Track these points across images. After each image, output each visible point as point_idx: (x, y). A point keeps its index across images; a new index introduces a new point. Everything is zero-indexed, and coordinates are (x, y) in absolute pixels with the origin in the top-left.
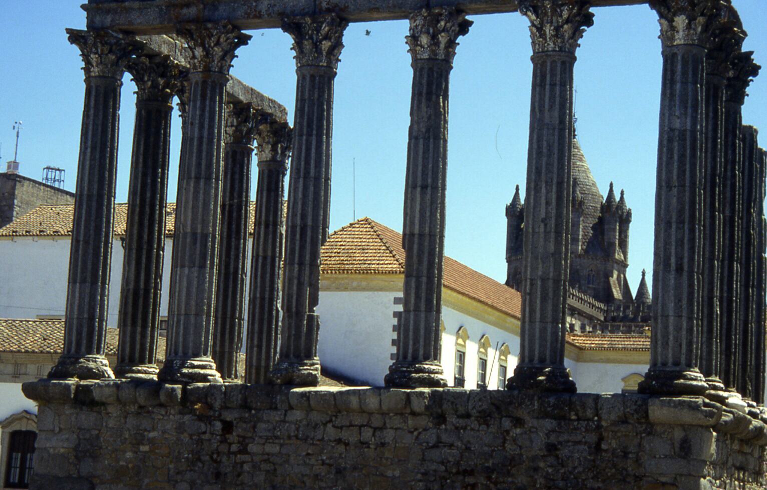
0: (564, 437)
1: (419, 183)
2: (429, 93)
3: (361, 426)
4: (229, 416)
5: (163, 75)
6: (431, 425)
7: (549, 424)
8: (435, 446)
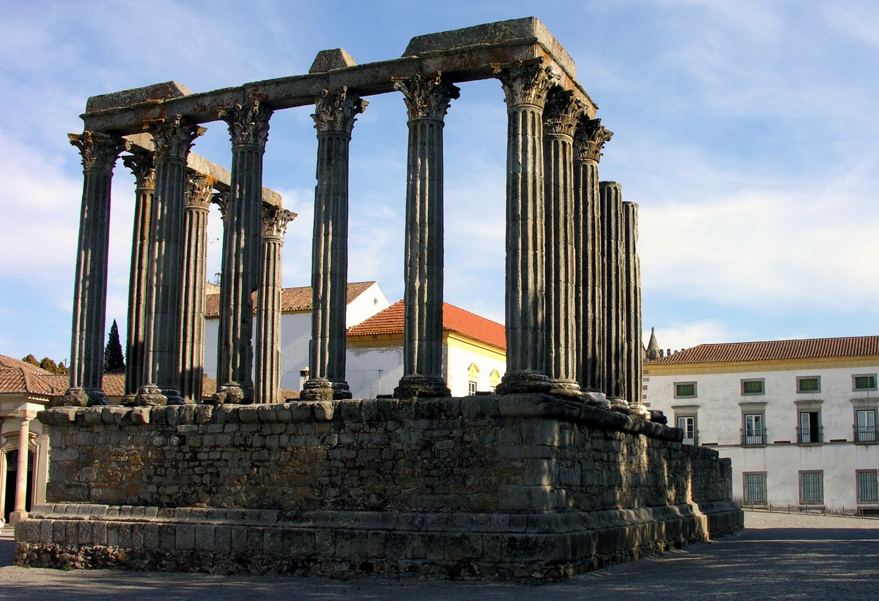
0: (436, 433)
2: (329, 159)
4: (182, 428)
6: (332, 430)
7: (423, 423)
8: (336, 447)
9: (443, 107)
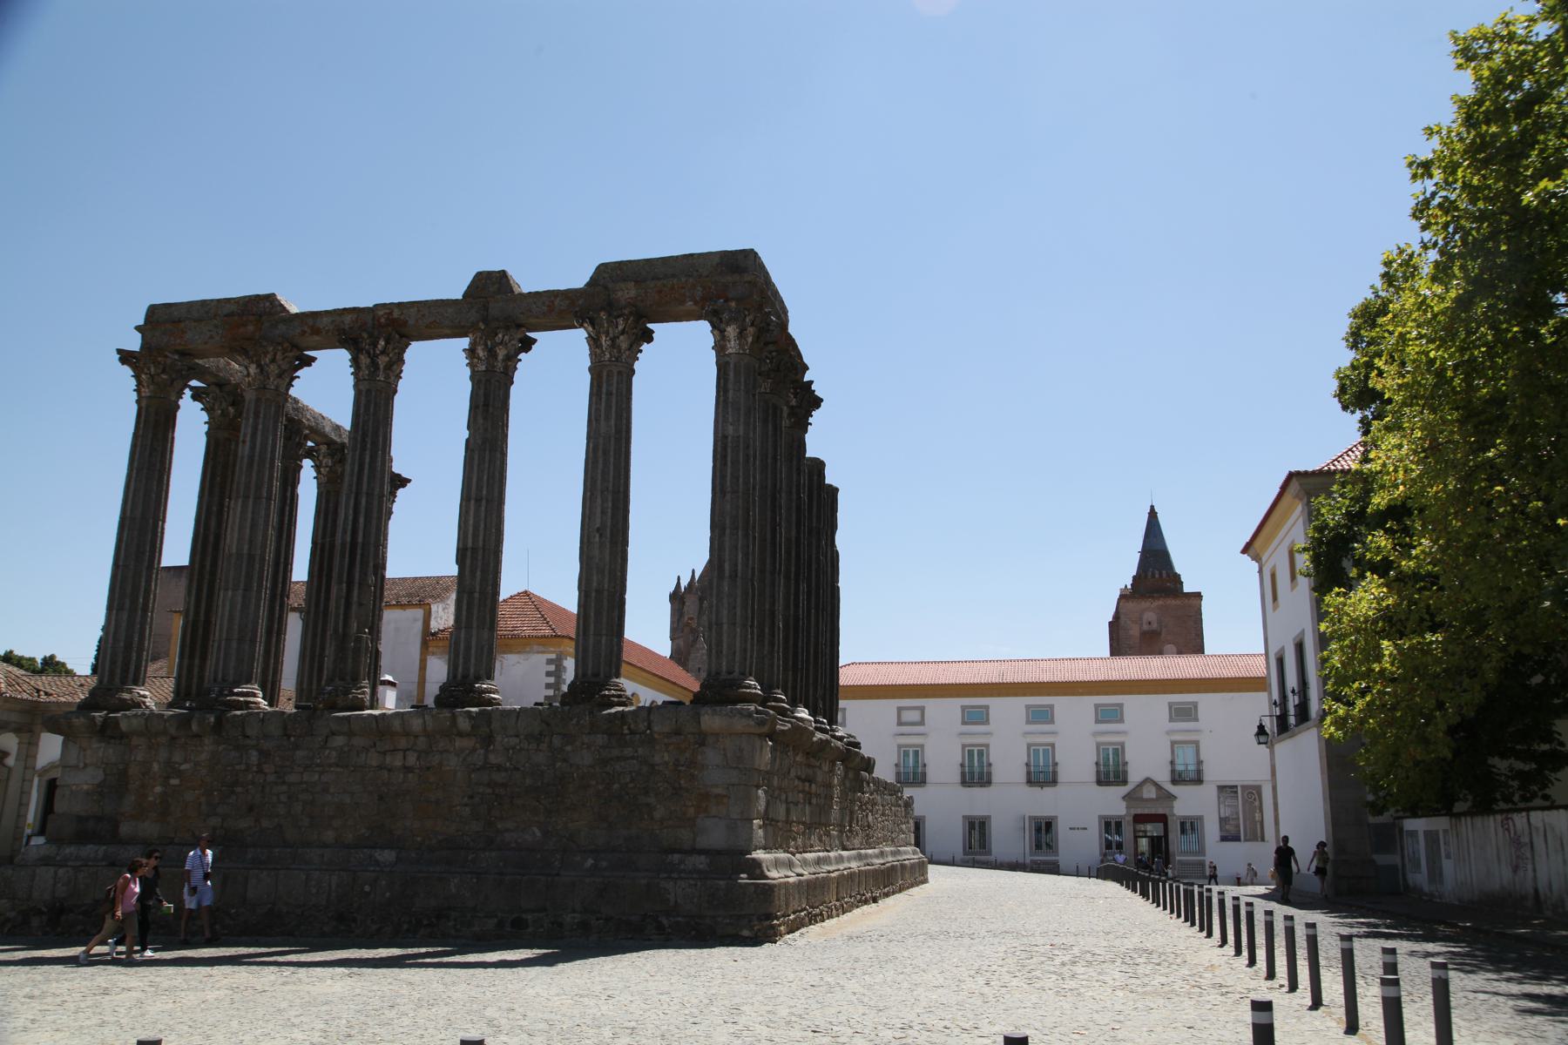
0: (616, 752)
2: (486, 405)
3: (405, 751)
5: (233, 404)
7: (600, 739)
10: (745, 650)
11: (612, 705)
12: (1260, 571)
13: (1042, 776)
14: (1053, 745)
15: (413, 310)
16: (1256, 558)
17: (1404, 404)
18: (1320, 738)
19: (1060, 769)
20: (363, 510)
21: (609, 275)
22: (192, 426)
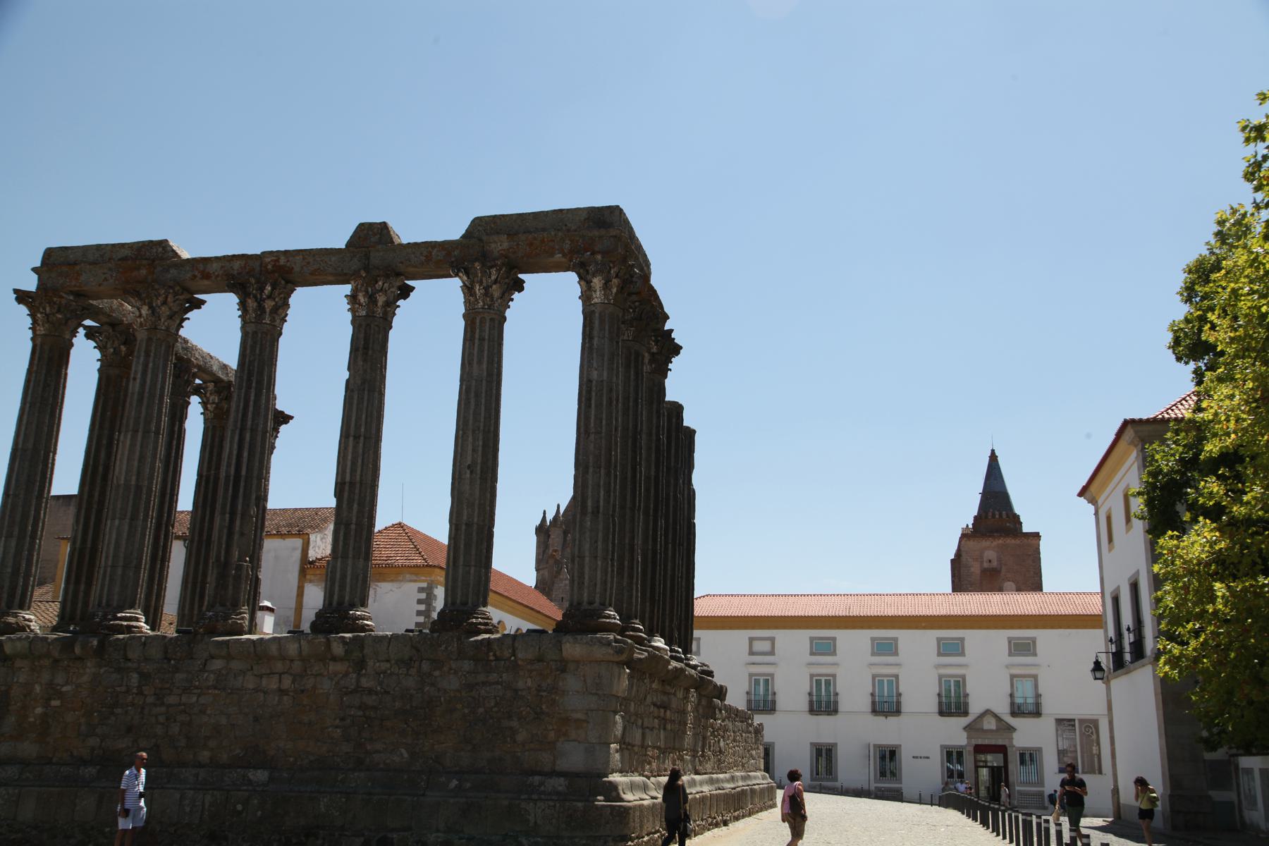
0: (481, 678)
1: (352, 432)
2: (366, 348)
3: (280, 674)
5: (124, 344)
7: (467, 665)
9: (506, 300)
10: (605, 582)
11: (479, 633)
12: (1096, 514)
13: (886, 705)
14: (897, 677)
15: (299, 258)
16: (1093, 501)
17: (1236, 356)
18: (1155, 676)
19: (903, 700)
20: (247, 446)
21: (483, 228)
22: (85, 360)
